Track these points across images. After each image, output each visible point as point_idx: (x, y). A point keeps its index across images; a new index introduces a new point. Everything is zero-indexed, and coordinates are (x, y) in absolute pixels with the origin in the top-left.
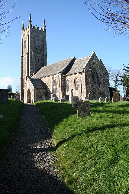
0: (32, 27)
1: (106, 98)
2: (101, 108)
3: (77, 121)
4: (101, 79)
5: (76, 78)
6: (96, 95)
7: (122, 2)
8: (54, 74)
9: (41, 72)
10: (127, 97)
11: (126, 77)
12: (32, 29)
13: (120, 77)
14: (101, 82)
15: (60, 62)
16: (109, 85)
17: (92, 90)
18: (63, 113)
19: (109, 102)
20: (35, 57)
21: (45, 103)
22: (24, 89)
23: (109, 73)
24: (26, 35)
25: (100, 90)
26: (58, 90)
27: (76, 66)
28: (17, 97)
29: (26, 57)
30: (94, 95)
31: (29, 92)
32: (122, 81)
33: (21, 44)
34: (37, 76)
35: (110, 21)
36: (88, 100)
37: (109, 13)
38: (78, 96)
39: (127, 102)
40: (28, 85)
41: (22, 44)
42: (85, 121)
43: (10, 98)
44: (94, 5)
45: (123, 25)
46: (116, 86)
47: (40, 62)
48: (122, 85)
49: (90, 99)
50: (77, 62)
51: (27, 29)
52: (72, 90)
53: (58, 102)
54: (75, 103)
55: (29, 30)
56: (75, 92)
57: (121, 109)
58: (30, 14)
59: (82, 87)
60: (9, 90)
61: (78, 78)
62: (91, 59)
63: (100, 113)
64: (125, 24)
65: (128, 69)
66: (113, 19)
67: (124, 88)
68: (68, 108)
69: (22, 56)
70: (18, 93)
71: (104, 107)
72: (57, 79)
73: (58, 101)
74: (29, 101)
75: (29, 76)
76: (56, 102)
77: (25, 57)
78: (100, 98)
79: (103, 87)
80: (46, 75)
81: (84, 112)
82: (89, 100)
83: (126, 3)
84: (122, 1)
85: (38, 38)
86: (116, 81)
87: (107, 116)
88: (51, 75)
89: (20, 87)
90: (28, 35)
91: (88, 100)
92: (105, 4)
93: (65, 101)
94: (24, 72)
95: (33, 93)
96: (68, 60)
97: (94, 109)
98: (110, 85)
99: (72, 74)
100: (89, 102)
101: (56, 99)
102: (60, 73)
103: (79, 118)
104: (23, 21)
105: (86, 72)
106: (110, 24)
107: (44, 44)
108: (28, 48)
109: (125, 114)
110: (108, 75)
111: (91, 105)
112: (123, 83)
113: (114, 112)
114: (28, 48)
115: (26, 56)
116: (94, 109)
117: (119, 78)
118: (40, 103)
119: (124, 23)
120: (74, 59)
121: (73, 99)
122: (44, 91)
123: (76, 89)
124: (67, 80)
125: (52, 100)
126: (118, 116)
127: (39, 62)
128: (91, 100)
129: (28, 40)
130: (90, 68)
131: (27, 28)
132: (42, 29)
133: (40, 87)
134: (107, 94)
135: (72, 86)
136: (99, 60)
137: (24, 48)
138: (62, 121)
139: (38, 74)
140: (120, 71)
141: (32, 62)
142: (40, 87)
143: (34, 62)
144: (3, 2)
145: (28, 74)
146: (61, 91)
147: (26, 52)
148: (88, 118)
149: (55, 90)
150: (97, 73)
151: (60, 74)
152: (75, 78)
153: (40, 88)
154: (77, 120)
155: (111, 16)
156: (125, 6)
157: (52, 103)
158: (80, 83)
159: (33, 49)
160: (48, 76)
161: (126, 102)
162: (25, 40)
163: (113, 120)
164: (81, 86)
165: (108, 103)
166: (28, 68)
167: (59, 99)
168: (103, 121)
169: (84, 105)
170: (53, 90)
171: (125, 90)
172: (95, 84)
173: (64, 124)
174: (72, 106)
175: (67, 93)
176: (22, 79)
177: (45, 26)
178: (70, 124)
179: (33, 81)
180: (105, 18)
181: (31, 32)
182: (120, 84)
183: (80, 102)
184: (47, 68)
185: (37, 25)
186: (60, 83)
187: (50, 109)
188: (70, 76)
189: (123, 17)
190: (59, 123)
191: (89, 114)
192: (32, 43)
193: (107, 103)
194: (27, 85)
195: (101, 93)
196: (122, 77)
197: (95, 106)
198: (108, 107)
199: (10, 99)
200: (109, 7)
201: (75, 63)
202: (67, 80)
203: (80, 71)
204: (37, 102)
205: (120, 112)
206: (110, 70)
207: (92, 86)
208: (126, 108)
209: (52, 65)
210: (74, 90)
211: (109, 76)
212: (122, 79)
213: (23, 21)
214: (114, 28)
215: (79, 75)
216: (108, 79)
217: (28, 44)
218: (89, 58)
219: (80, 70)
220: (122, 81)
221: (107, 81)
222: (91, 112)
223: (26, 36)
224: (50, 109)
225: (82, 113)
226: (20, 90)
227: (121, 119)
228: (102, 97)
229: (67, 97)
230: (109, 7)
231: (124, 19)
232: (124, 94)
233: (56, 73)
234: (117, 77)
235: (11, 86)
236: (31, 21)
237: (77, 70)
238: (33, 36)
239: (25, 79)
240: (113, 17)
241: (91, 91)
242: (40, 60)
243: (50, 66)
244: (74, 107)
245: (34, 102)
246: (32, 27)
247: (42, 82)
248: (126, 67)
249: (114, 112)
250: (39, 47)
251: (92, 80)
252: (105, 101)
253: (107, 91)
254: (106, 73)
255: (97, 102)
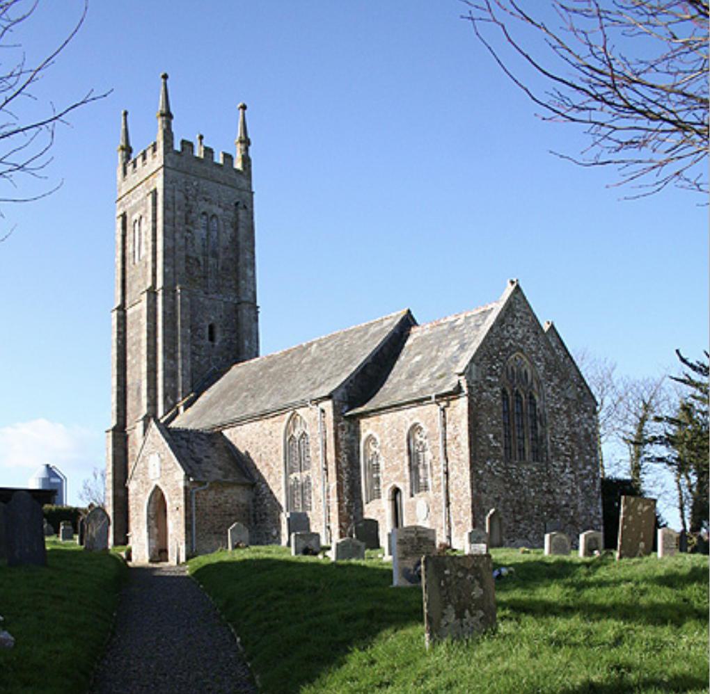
0: (178, 147)
1: (582, 537)
2: (552, 593)
3: (423, 665)
4: (557, 432)
5: (415, 428)
6: (530, 518)
7: (671, 9)
8: (294, 407)
9: (223, 394)
10: (696, 528)
11: (692, 421)
12: (177, 158)
13: (658, 419)
14: (555, 450)
15: (328, 339)
16: (598, 465)
17: (507, 490)
18: (348, 619)
19: (601, 558)
20: (193, 309)
21: (245, 562)
22: (132, 486)
23: (598, 400)
24: (142, 193)
25: (550, 492)
26: (318, 491)
27: (418, 358)
28: (93, 531)
29: (139, 312)
30: (519, 517)
31: (158, 503)
32: (669, 441)
33: (116, 242)
34: (202, 413)
35: (604, 114)
36: (482, 548)
37: (601, 73)
38: (427, 525)
39: (698, 557)
40: (154, 463)
41: (119, 239)
42: (470, 663)
43: (53, 538)
44: (517, 27)
45: (678, 136)
46: (636, 469)
47: (219, 337)
48: (670, 464)
49: (496, 539)
50: (424, 339)
51: (149, 158)
52: (396, 491)
53: (320, 556)
54: (409, 564)
55: (156, 161)
56: (414, 506)
57: (665, 596)
58: (165, 77)
59: (451, 474)
60: (50, 492)
61: (430, 426)
62: (500, 321)
63: (552, 619)
64: (685, 129)
65: (705, 380)
66: (621, 102)
67: (684, 481)
68: (370, 590)
69: (122, 309)
70: (97, 512)
71: (571, 585)
72: (314, 432)
73: (316, 554)
74: (160, 553)
75: (160, 413)
76: (309, 559)
77: (138, 311)
78: (547, 537)
79: (567, 476)
80: (251, 411)
81: (460, 615)
82: (491, 545)
83: (695, 13)
84: (670, 5)
85: (204, 207)
86: (639, 442)
87: (589, 633)
88: (281, 411)
89: (110, 477)
90: (155, 193)
91: (482, 548)
92: (579, 21)
93: (358, 553)
94: (129, 393)
95: (182, 509)
96: (373, 330)
97: (517, 594)
98: (605, 464)
99: (397, 406)
100: (488, 556)
101: (310, 544)
102: (329, 397)
103: (433, 646)
104: (126, 114)
105: (470, 396)
106: (605, 130)
107: (240, 239)
108: (154, 260)
109: (690, 625)
110: (595, 413)
111: (500, 576)
112: (676, 453)
113: (626, 612)
114: (154, 260)
115: (144, 304)
116: (517, 594)
117: (655, 429)
118: (221, 565)
119: (681, 126)
120: (407, 323)
121: (401, 542)
122: (238, 496)
123: (418, 486)
124: (370, 438)
125: (285, 547)
126: (646, 633)
127: (212, 339)
128: (500, 545)
129: (155, 220)
130: (492, 372)
131: (149, 152)
132: (227, 157)
133: (217, 474)
134: (586, 512)
135: (393, 472)
136: (546, 327)
137: (129, 262)
138: (340, 665)
139: (210, 404)
140: (658, 386)
141: (175, 338)
142: (217, 474)
143: (183, 337)
144: (14, 12)
145: (153, 403)
146: (334, 500)
147: (140, 282)
148: (486, 647)
149: (299, 491)
150: (532, 397)
151: (328, 405)
152: (410, 425)
153: (217, 482)
154: (425, 655)
155: (608, 89)
156: (685, 32)
157: (288, 564)
158: (441, 454)
159: (181, 268)
160: (264, 415)
161: (690, 560)
162: (136, 216)
163: (622, 654)
164: (447, 473)
165: (592, 566)
166: (152, 371)
167: (323, 543)
168: (567, 665)
169: (460, 574)
170: (290, 490)
171: (685, 490)
172: (523, 458)
173: (352, 680)
174: (397, 581)
175: (370, 511)
176: (120, 435)
177: (246, 142)
178: (385, 679)
179: (181, 442)
180: (579, 99)
181: (170, 172)
182: (660, 460)
183: (442, 560)
184: (255, 373)
185: (201, 138)
186: (331, 456)
187: (277, 598)
188: (386, 418)
189: (678, 93)
190: (323, 674)
191: (489, 625)
192: (177, 236)
193: (587, 565)
194: (146, 468)
195: (555, 510)
196: (672, 421)
197: (524, 579)
198: (590, 585)
199: (54, 542)
200: (597, 40)
201: (409, 342)
202: (370, 438)
203: (442, 387)
204: (203, 560)
205: (659, 616)
206: (604, 383)
207: (506, 468)
208: (692, 590)
209: (286, 353)
210: (405, 498)
211: (602, 414)
212: (672, 430)
213: (126, 114)
214: (630, 154)
215: (433, 410)
216: (595, 433)
217: (155, 240)
218: (492, 318)
219: (439, 382)
220: (669, 441)
221: (590, 443)
222: (500, 613)
223: (142, 195)
224: (277, 598)
225: (451, 616)
226: (110, 494)
227: (668, 653)
228: (562, 531)
229: (368, 533)
230: (597, 40)
231: (683, 103)
232: (682, 516)
233: (306, 396)
234: (643, 420)
235: (61, 469)
236: (167, 115)
237: (423, 380)
238: (179, 196)
239: (135, 430)
240: (622, 91)
241: (498, 499)
242: (218, 330)
243: (273, 361)
244: (409, 584)
245: (188, 558)
246: (178, 147)
247: (230, 448)
248: (691, 366)
249: (626, 612)
250: (215, 255)
251: (508, 437)
252: (580, 555)
253: (588, 497)
254: (585, 401)
255: (532, 556)
